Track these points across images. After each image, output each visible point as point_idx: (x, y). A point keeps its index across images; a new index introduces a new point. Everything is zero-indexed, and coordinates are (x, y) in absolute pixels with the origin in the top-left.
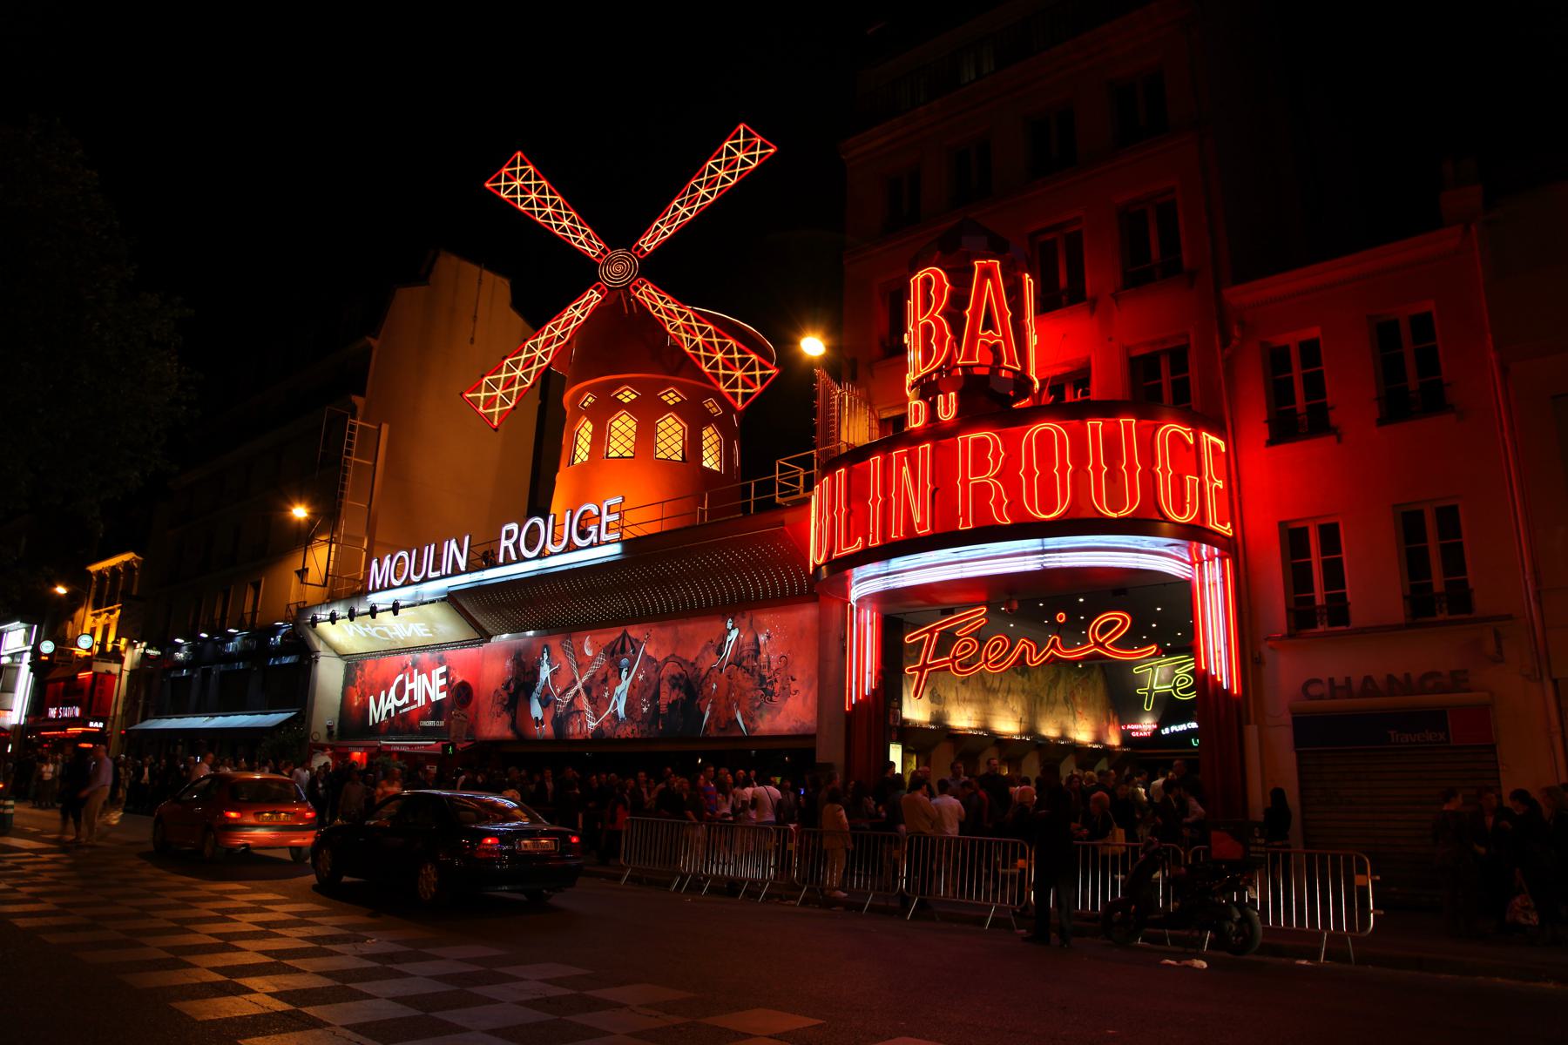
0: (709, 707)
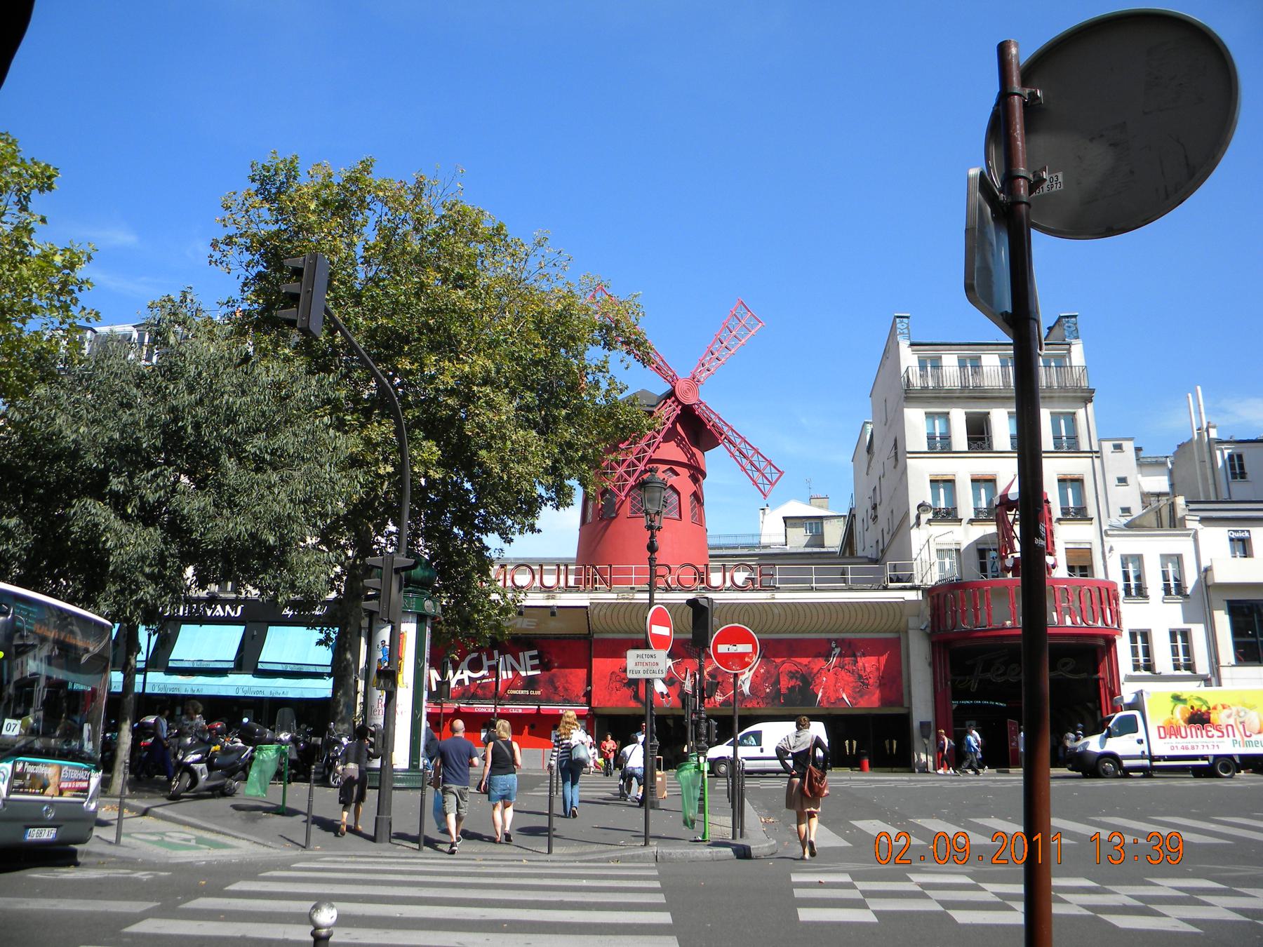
0: (821, 690)
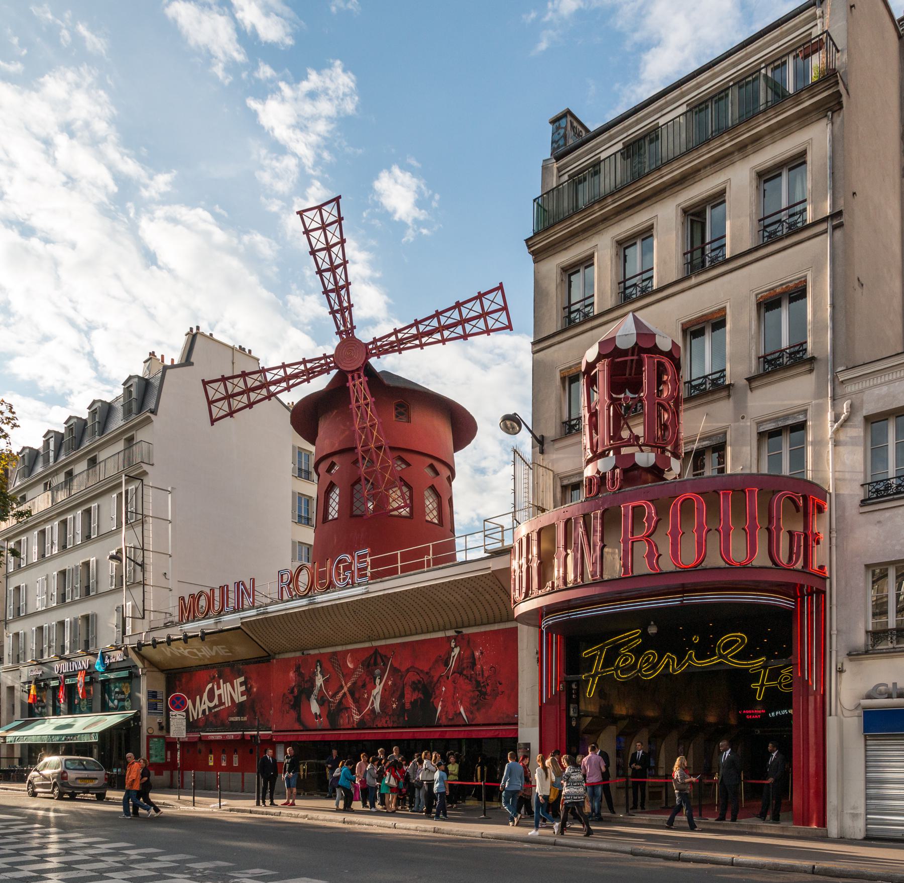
0: (440, 704)
